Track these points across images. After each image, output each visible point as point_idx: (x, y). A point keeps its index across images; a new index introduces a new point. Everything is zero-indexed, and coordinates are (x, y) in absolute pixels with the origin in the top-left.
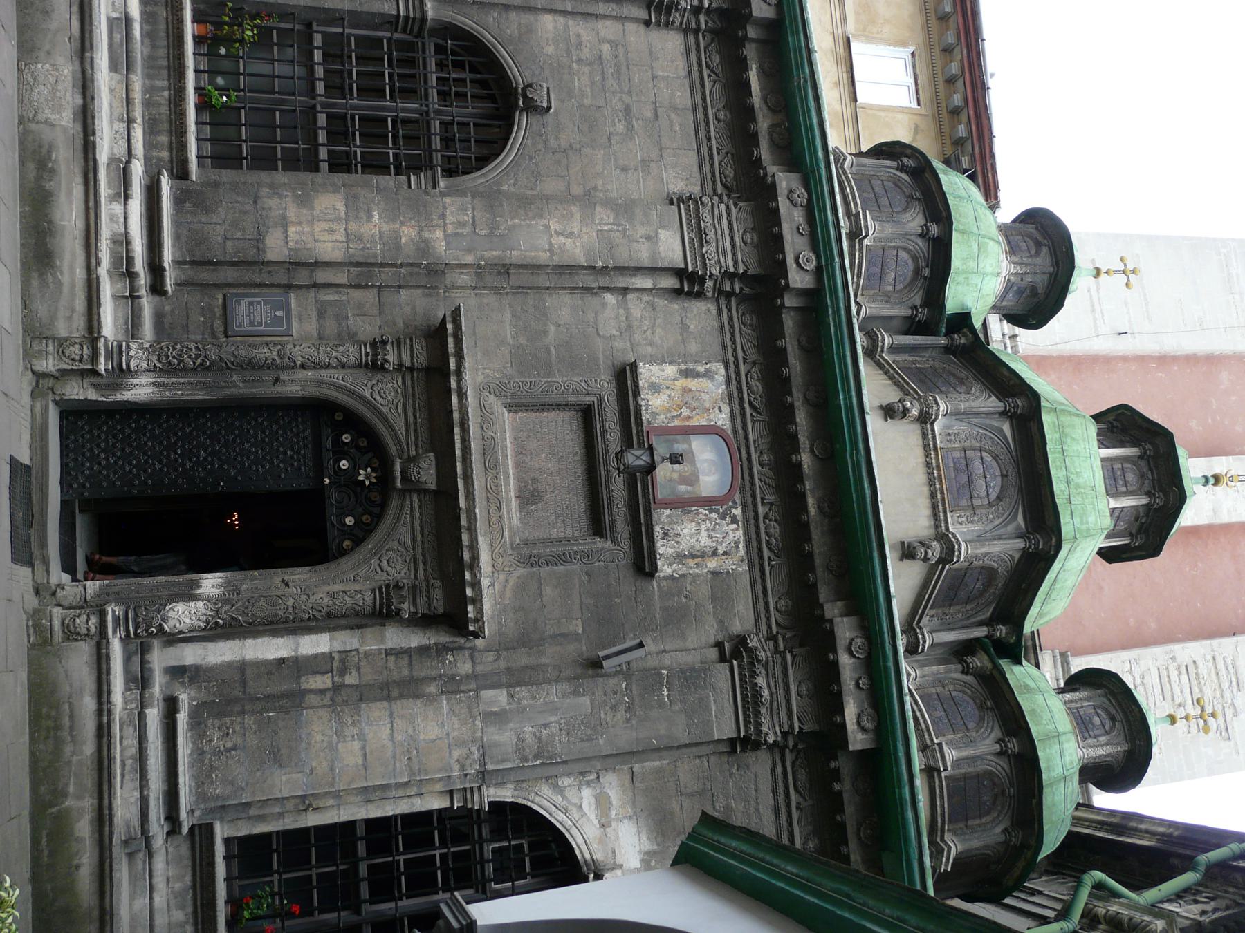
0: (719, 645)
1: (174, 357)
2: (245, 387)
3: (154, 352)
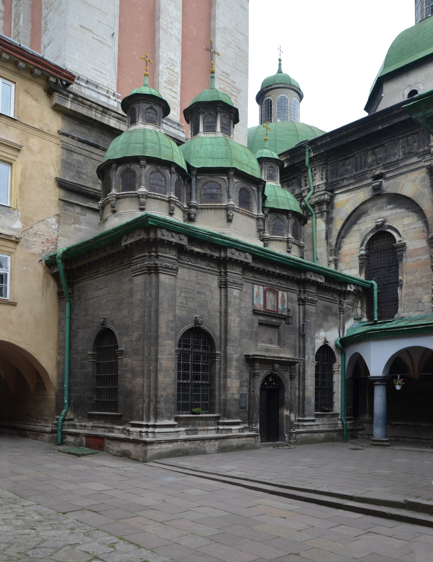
0: (299, 304)
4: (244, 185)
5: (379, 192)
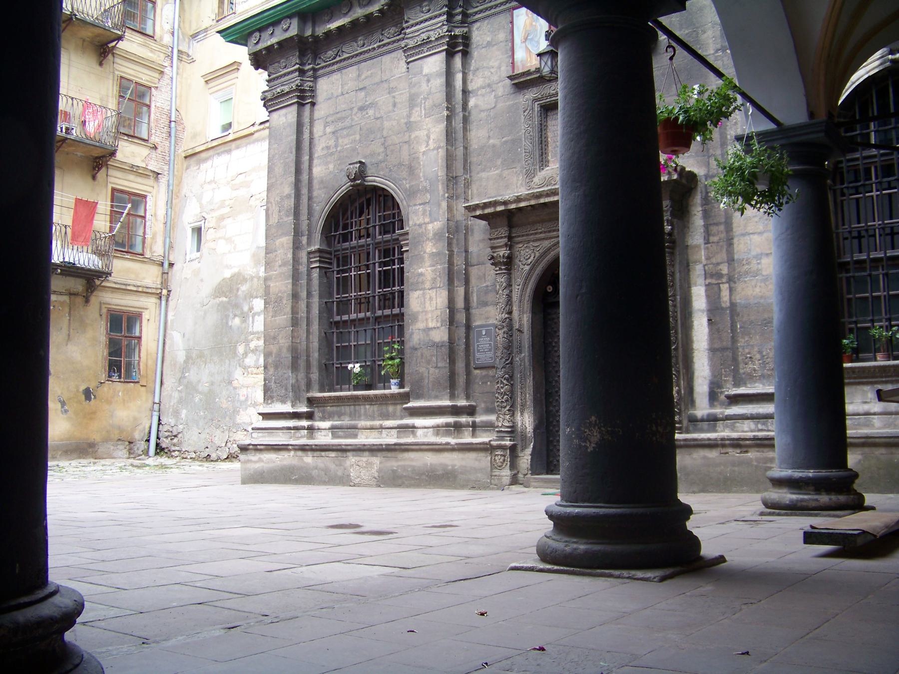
1: (502, 398)
2: (525, 352)
3: (500, 411)
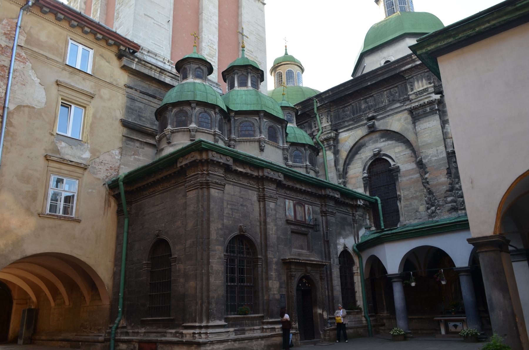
0: (322, 216)
4: (272, 124)
5: (373, 129)
